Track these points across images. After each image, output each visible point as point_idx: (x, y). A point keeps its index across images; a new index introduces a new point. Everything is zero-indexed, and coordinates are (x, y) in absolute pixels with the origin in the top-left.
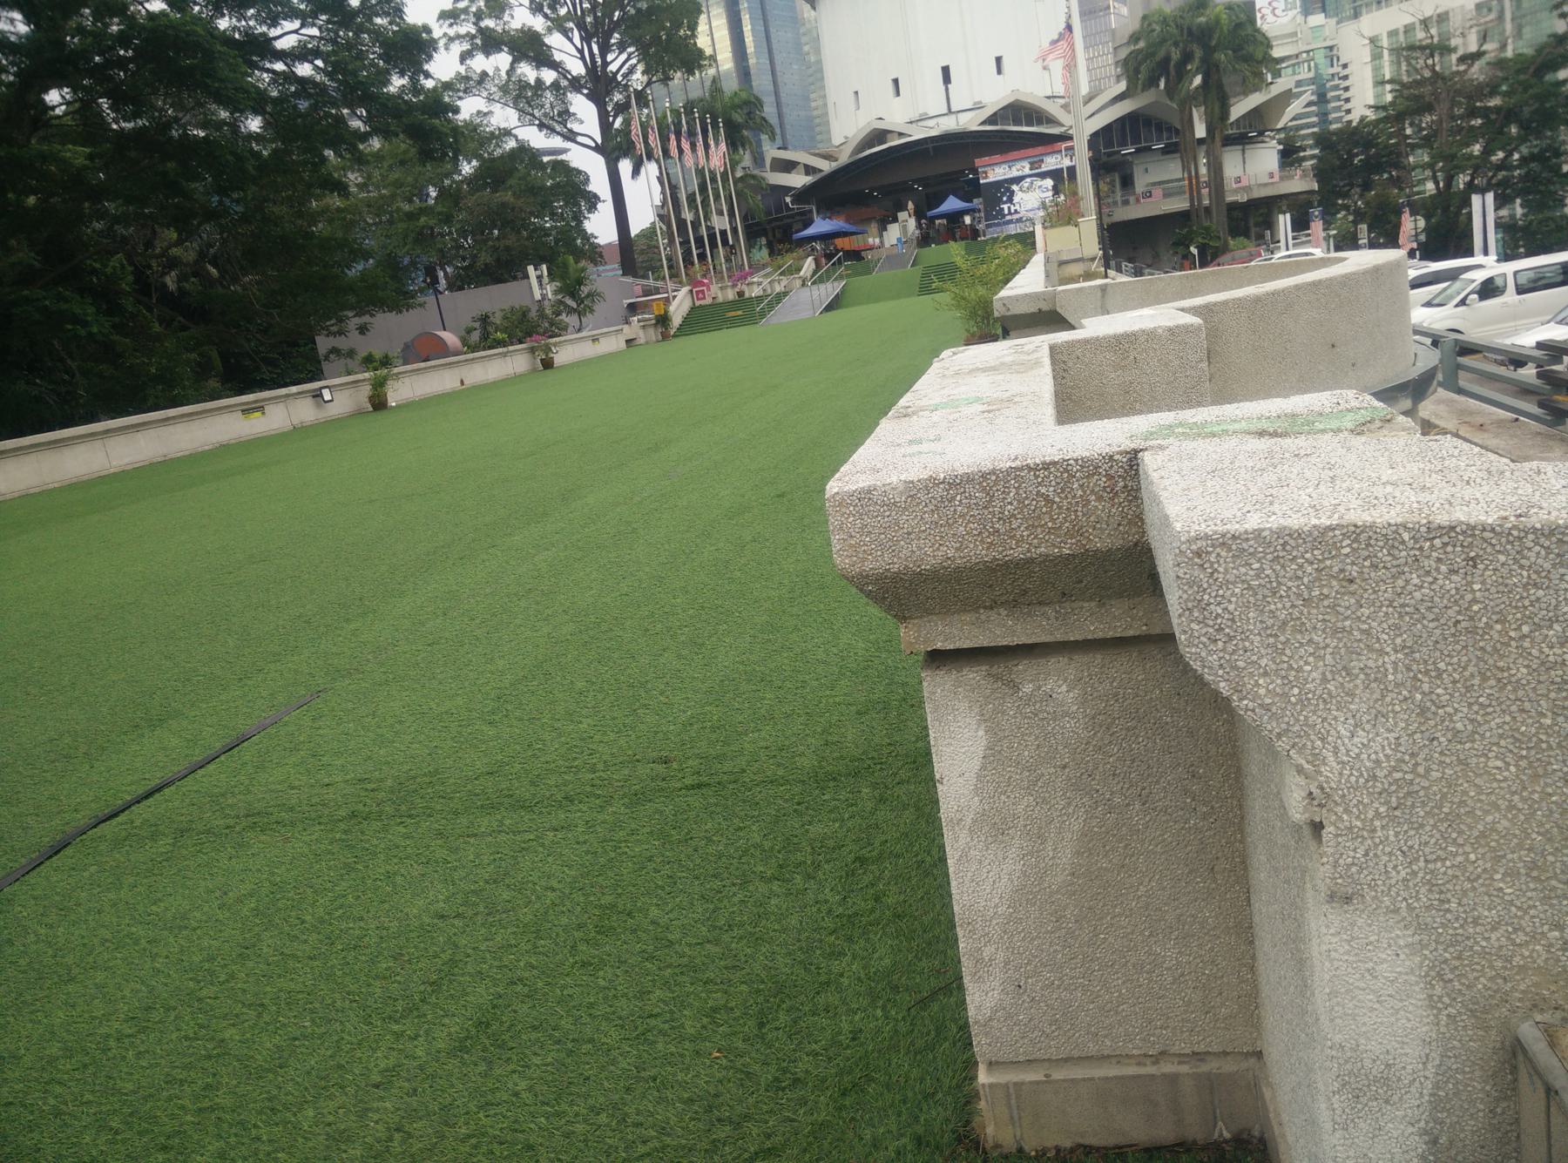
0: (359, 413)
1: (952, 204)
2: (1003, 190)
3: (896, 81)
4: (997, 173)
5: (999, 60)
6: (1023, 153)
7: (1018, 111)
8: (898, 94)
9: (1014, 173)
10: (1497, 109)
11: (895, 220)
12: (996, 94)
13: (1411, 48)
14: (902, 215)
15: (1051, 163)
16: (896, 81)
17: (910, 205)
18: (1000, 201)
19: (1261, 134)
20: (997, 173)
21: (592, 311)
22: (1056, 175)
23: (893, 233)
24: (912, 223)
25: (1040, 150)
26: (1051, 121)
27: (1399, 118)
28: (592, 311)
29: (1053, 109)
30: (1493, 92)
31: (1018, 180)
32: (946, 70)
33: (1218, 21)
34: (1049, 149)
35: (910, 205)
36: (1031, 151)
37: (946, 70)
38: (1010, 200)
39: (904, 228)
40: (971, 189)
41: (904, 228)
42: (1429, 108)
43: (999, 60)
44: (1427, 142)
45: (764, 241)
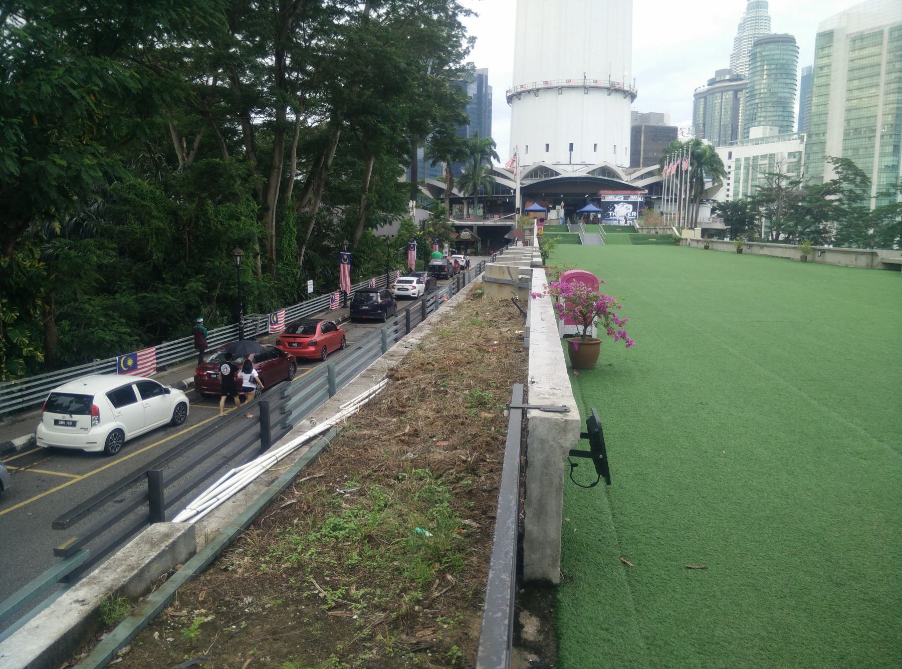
0: (732, 253)
1: (590, 207)
2: (611, 205)
3: (547, 145)
4: (609, 198)
5: (595, 145)
6: (622, 192)
7: (605, 170)
8: (547, 150)
9: (617, 199)
10: (803, 207)
11: (554, 208)
12: (598, 160)
13: (770, 174)
14: (558, 207)
15: (633, 198)
16: (547, 145)
17: (562, 203)
18: (608, 210)
19: (708, 200)
20: (609, 198)
21: (391, 224)
22: (634, 204)
23: (552, 215)
24: (562, 212)
25: (629, 192)
26: (619, 177)
27: (756, 203)
28: (391, 224)
29: (619, 171)
30: (804, 200)
31: (618, 203)
32: (571, 145)
33: (705, 152)
34: (633, 192)
35: (562, 203)
36: (625, 192)
37: (571, 145)
38: (613, 210)
39: (558, 214)
40: (598, 201)
41: (558, 214)
42: (773, 201)
43: (595, 145)
44: (769, 217)
45: (482, 205)
